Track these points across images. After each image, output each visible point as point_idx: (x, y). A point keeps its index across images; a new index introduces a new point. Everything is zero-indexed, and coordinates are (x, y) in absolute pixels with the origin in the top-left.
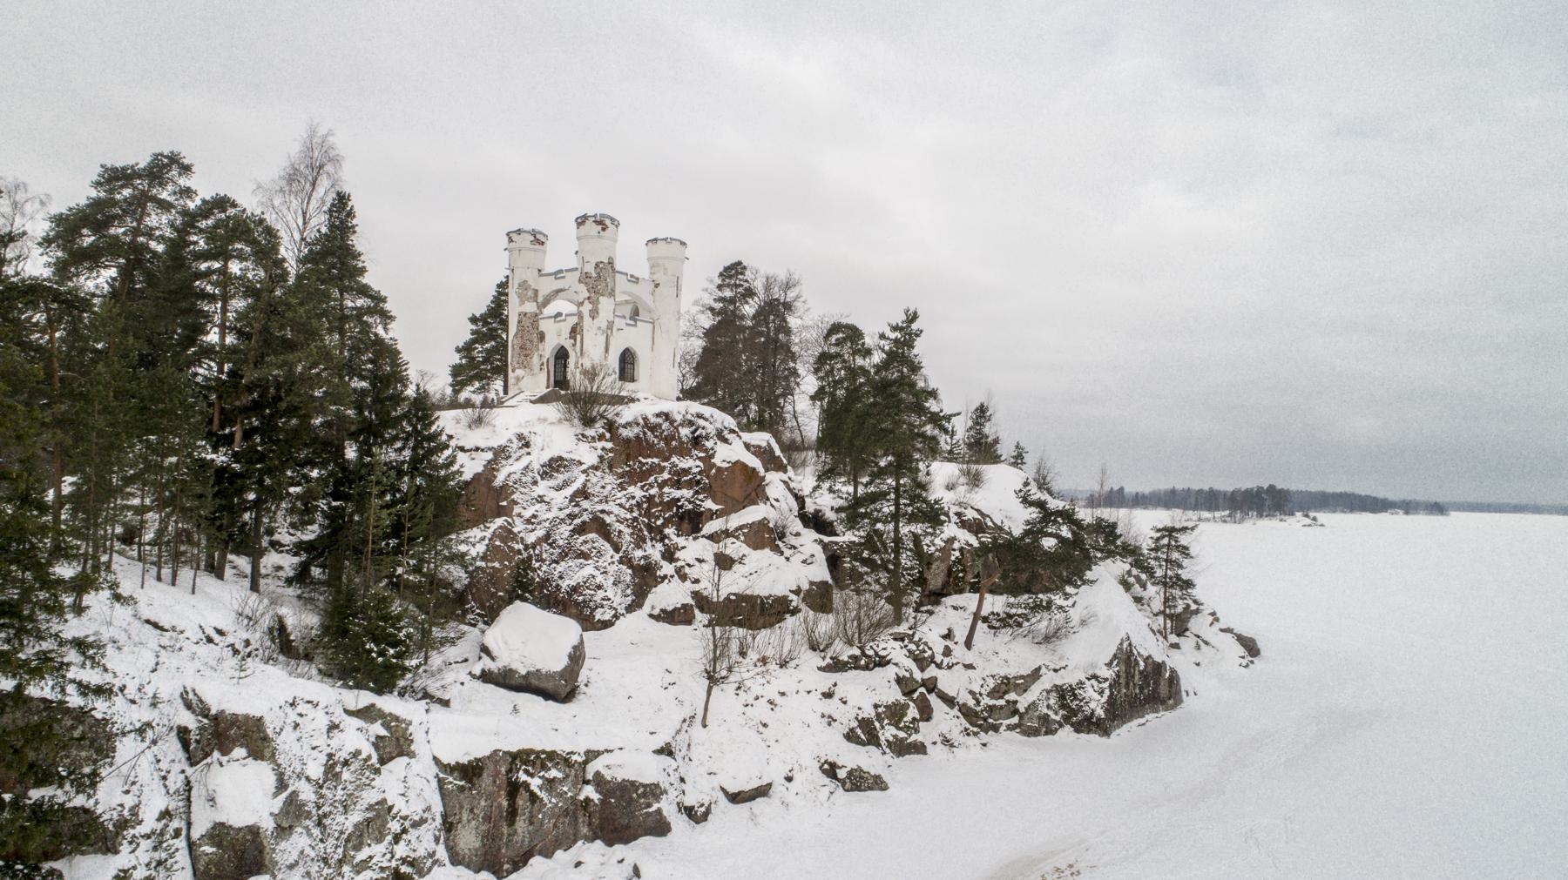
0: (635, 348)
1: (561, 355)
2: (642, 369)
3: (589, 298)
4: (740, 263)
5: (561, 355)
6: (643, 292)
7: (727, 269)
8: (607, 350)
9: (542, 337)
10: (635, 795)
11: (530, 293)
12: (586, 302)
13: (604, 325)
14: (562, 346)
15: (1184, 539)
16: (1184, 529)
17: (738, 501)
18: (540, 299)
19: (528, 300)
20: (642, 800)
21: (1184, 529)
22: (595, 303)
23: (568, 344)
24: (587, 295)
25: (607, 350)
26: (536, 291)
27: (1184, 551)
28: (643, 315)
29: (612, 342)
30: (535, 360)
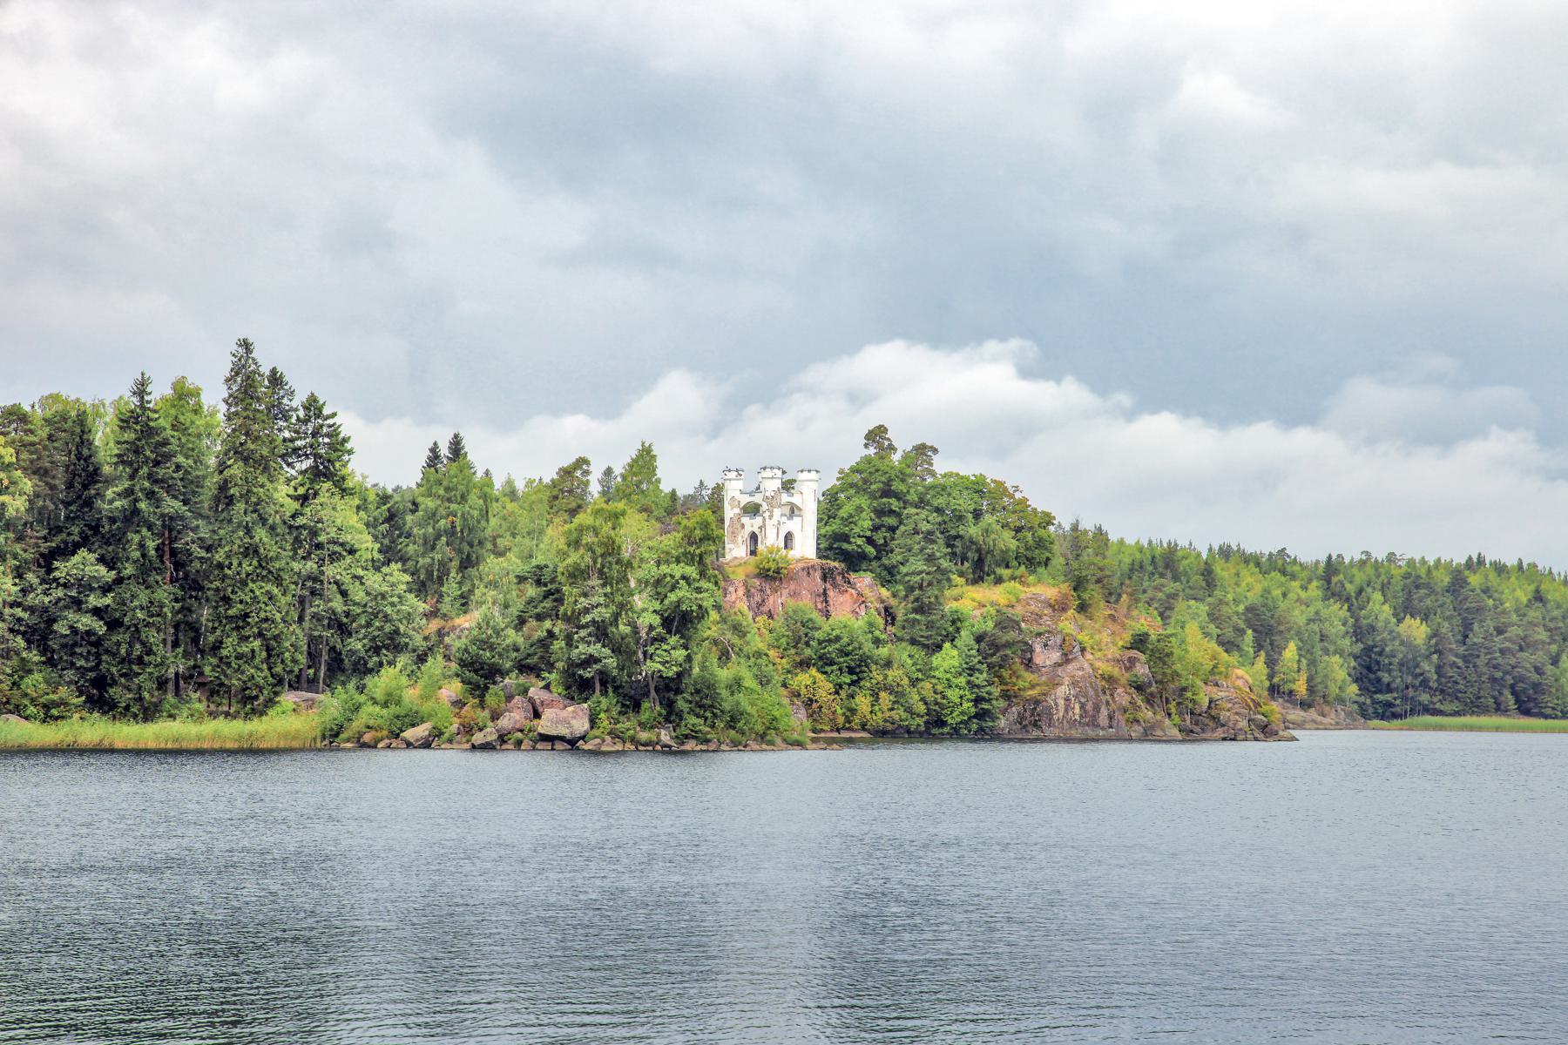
1: (754, 537)
5: (754, 537)
7: (870, 432)
9: (743, 526)
13: (776, 523)
22: (771, 512)
23: (757, 531)
30: (740, 539)
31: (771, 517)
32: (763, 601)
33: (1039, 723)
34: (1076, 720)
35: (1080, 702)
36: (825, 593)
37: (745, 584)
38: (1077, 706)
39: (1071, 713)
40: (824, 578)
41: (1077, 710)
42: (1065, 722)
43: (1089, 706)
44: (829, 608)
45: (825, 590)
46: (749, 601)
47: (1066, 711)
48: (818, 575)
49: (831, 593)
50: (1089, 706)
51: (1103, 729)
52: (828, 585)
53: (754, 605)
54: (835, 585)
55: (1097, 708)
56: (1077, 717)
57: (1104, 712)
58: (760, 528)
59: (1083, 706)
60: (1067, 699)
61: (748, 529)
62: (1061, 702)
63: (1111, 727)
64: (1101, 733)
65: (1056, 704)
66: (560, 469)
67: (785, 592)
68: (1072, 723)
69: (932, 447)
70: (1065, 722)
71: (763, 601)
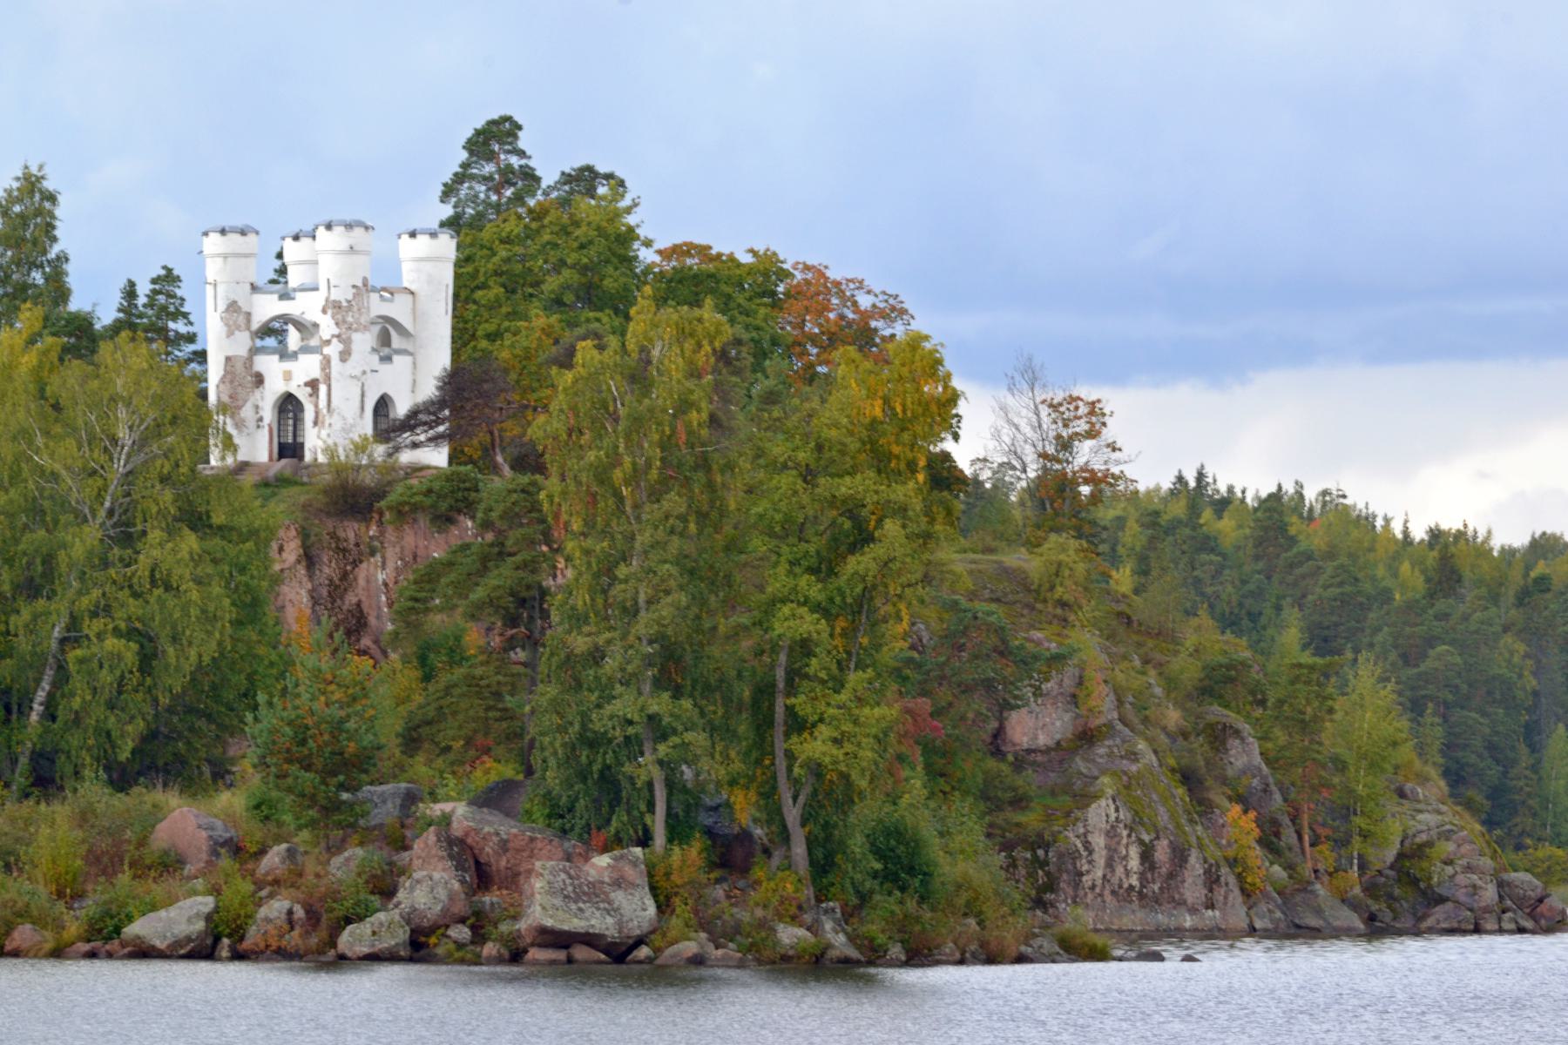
0: (391, 393)
3: (338, 336)
4: (508, 119)
5: (289, 405)
6: (398, 310)
7: (478, 133)
8: (362, 408)
9: (259, 380)
11: (241, 319)
12: (335, 340)
18: (255, 326)
19: (238, 328)
23: (302, 394)
24: (336, 331)
25: (362, 401)
26: (249, 315)
28: (396, 341)
29: (367, 394)
31: (345, 355)
32: (344, 576)
33: (1049, 896)
34: (1131, 887)
35: (1141, 842)
37: (304, 534)
38: (1134, 853)
39: (1120, 870)
41: (1134, 863)
42: (1107, 893)
43: (1162, 853)
46: (311, 577)
47: (1110, 864)
50: (1162, 853)
51: (1193, 910)
53: (324, 592)
55: (1180, 856)
56: (1134, 881)
57: (1195, 865)
58: (313, 384)
59: (1147, 855)
60: (1111, 833)
61: (275, 387)
62: (1099, 841)
64: (1188, 922)
65: (1087, 846)
67: (391, 553)
68: (1124, 895)
69: (609, 177)
70: (1107, 893)
71: (344, 576)
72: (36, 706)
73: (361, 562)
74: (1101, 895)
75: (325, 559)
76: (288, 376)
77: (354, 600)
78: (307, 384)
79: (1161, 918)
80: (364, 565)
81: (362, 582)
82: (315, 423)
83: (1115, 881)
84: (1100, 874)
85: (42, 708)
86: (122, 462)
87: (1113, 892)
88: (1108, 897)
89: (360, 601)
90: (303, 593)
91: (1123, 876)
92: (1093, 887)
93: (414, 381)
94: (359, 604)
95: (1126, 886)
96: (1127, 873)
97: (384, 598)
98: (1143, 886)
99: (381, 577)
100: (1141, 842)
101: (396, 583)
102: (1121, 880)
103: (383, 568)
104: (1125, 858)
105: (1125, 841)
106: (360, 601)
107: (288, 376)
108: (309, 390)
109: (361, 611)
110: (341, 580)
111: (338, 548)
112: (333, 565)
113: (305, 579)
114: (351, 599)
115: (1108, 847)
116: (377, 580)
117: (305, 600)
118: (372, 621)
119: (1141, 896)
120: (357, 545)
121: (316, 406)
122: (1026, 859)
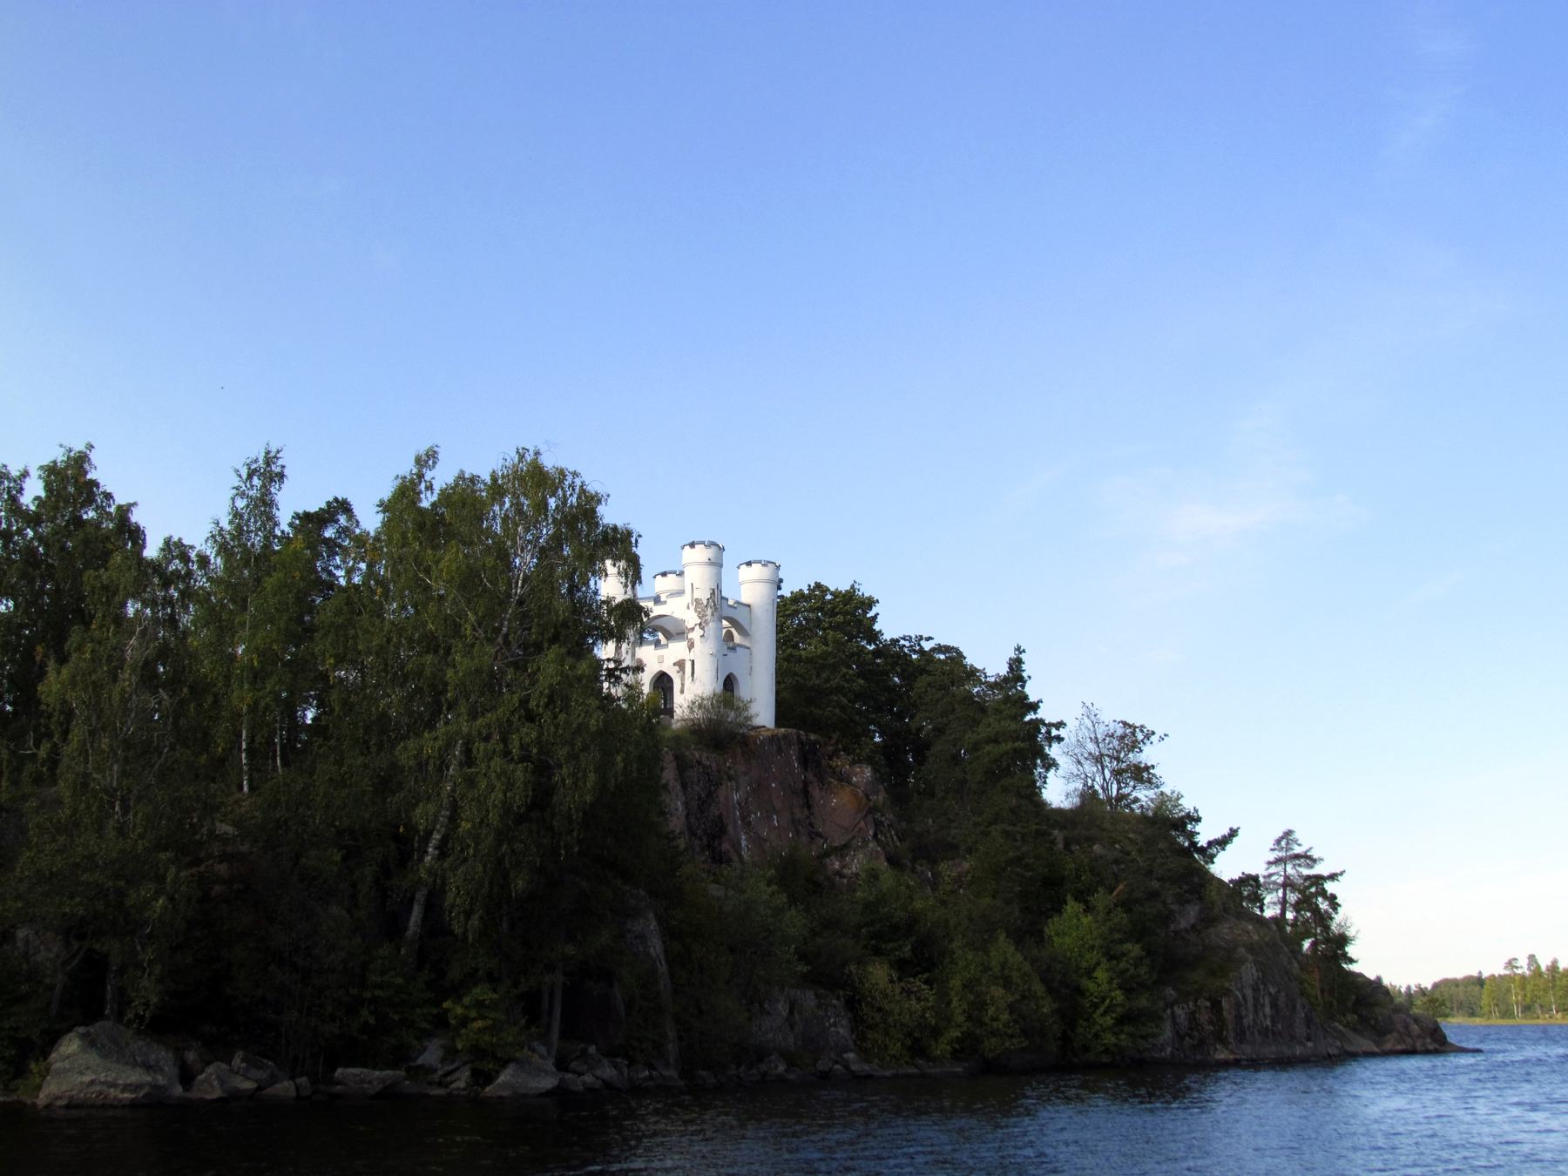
0: (735, 673)
2: (743, 691)
10: (827, 1024)
14: (665, 673)
15: (1330, 887)
16: (1333, 877)
17: (846, 830)
20: (833, 1029)
21: (1333, 877)
24: (699, 621)
27: (1332, 900)
32: (710, 794)
36: (806, 792)
39: (1261, 1014)
40: (805, 762)
41: (1268, 1010)
42: (1255, 1030)
44: (813, 820)
45: (805, 783)
47: (1256, 1012)
48: (793, 753)
49: (815, 792)
51: (1300, 1043)
52: (810, 777)
54: (821, 780)
56: (1269, 1023)
58: (680, 664)
59: (1274, 1005)
60: (1255, 989)
62: (1249, 992)
63: (1309, 1039)
66: (297, 516)
71: (710, 794)
72: (430, 850)
73: (721, 784)
74: (1253, 1033)
75: (695, 780)
76: (661, 661)
77: (717, 813)
78: (674, 664)
79: (1287, 1052)
80: (724, 787)
81: (722, 798)
82: (682, 692)
83: (1259, 1022)
84: (1251, 1017)
85: (437, 852)
86: (520, 585)
87: (1259, 1032)
88: (1256, 1034)
89: (721, 814)
90: (679, 803)
91: (1263, 1019)
92: (1249, 1027)
93: (751, 668)
94: (720, 816)
95: (1264, 1026)
96: (1265, 1016)
97: (738, 813)
98: (1273, 1026)
99: (736, 797)
100: (1270, 994)
101: (746, 803)
102: (1261, 1021)
103: (737, 791)
104: (1263, 1006)
105: (1262, 993)
106: (721, 814)
107: (661, 661)
108: (677, 668)
109: (722, 821)
110: (707, 797)
111: (704, 771)
112: (701, 784)
113: (680, 794)
114: (714, 811)
115: (1254, 998)
116: (733, 799)
117: (681, 809)
118: (730, 829)
119: (1273, 1033)
120: (719, 771)
121: (683, 679)
122: (1207, 1007)
